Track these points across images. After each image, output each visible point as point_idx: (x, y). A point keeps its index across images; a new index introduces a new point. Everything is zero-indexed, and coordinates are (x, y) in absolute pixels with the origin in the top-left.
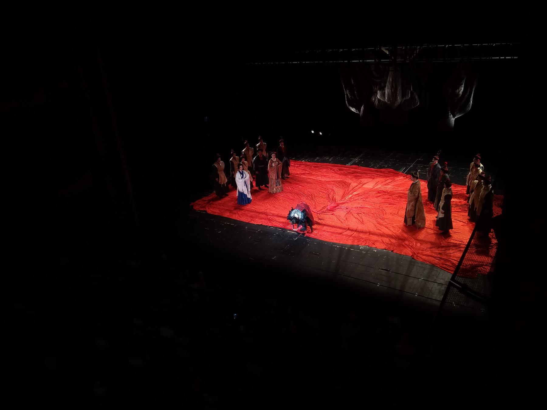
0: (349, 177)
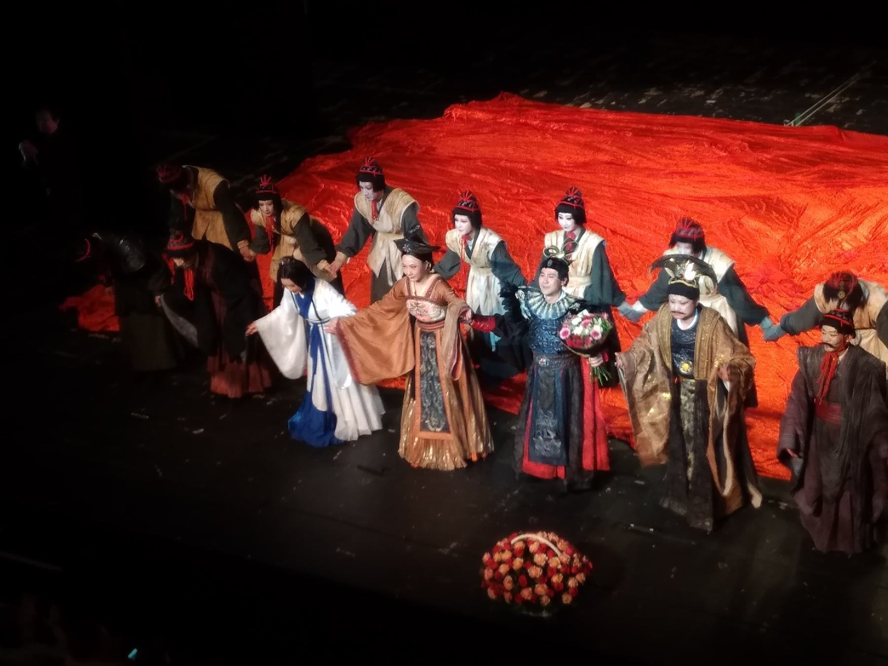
0: (799, 177)
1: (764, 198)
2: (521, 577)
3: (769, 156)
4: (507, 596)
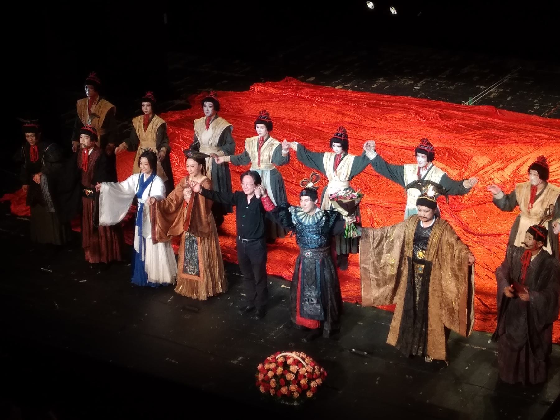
0: (470, 137)
1: (447, 149)
2: (281, 380)
3: (451, 123)
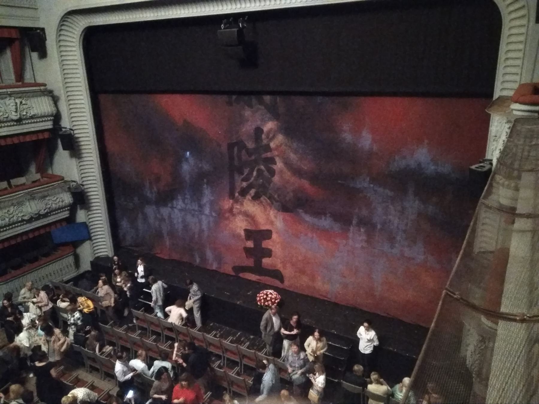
4: (262, 304)
